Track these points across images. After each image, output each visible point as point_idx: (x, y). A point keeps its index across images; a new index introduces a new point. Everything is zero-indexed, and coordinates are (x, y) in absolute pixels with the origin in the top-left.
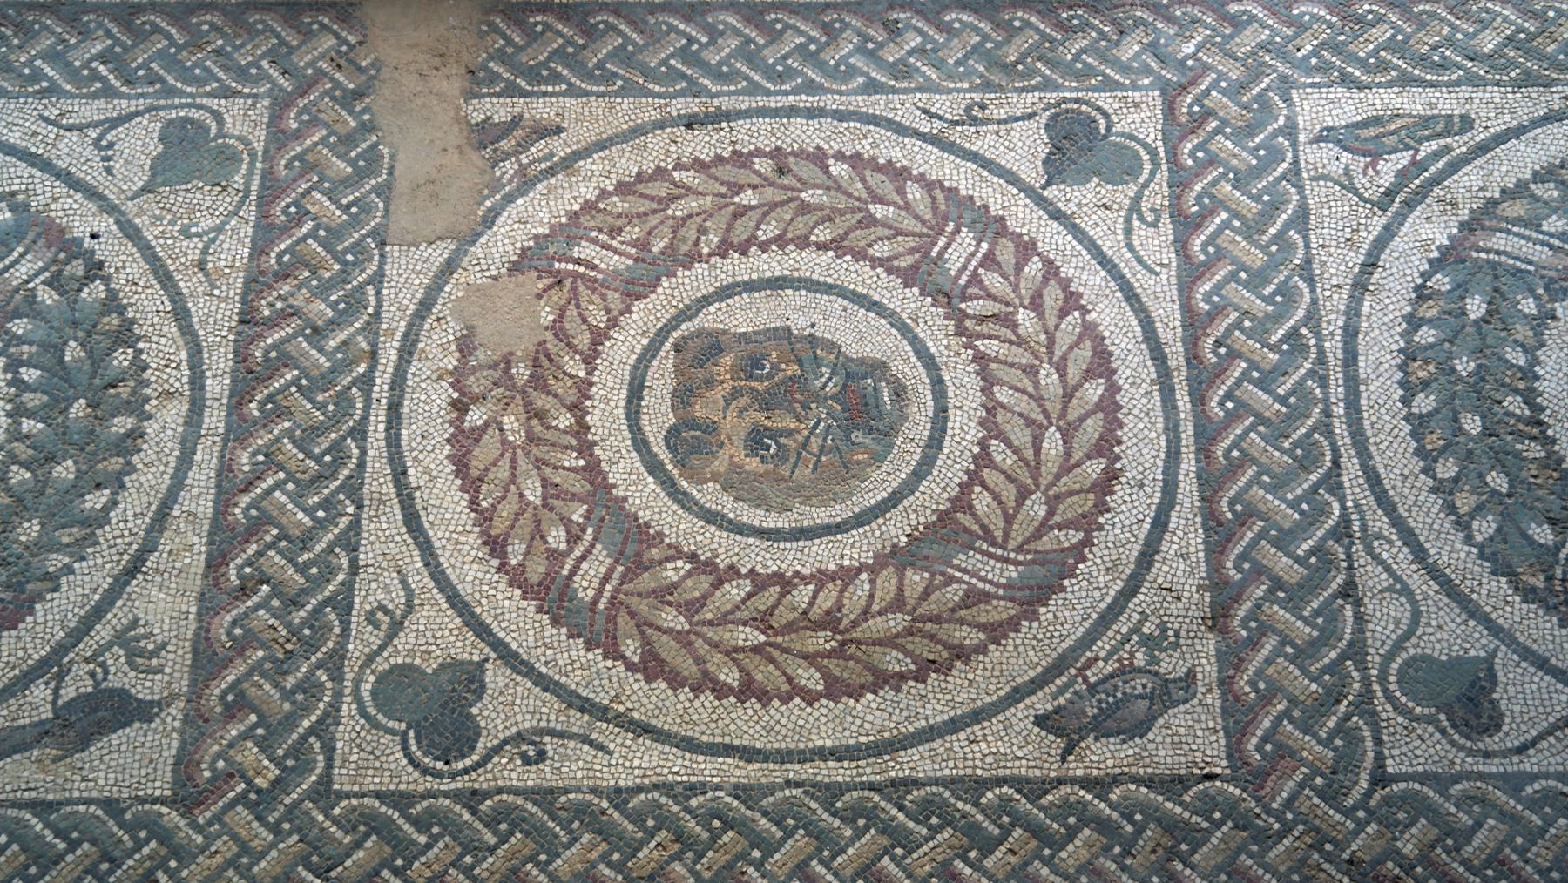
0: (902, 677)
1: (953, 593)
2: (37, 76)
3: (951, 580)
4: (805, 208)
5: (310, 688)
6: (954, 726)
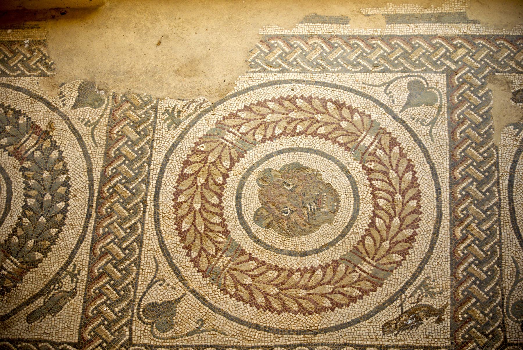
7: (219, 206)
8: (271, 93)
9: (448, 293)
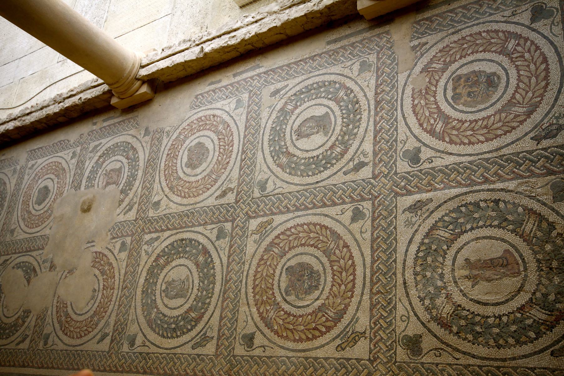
0: (501, 135)
1: (512, 116)
2: (340, 60)
3: (511, 113)
4: (477, 45)
5: (392, 156)
6: (513, 143)
7: (176, 163)
8: (196, 117)
9: (237, 181)
